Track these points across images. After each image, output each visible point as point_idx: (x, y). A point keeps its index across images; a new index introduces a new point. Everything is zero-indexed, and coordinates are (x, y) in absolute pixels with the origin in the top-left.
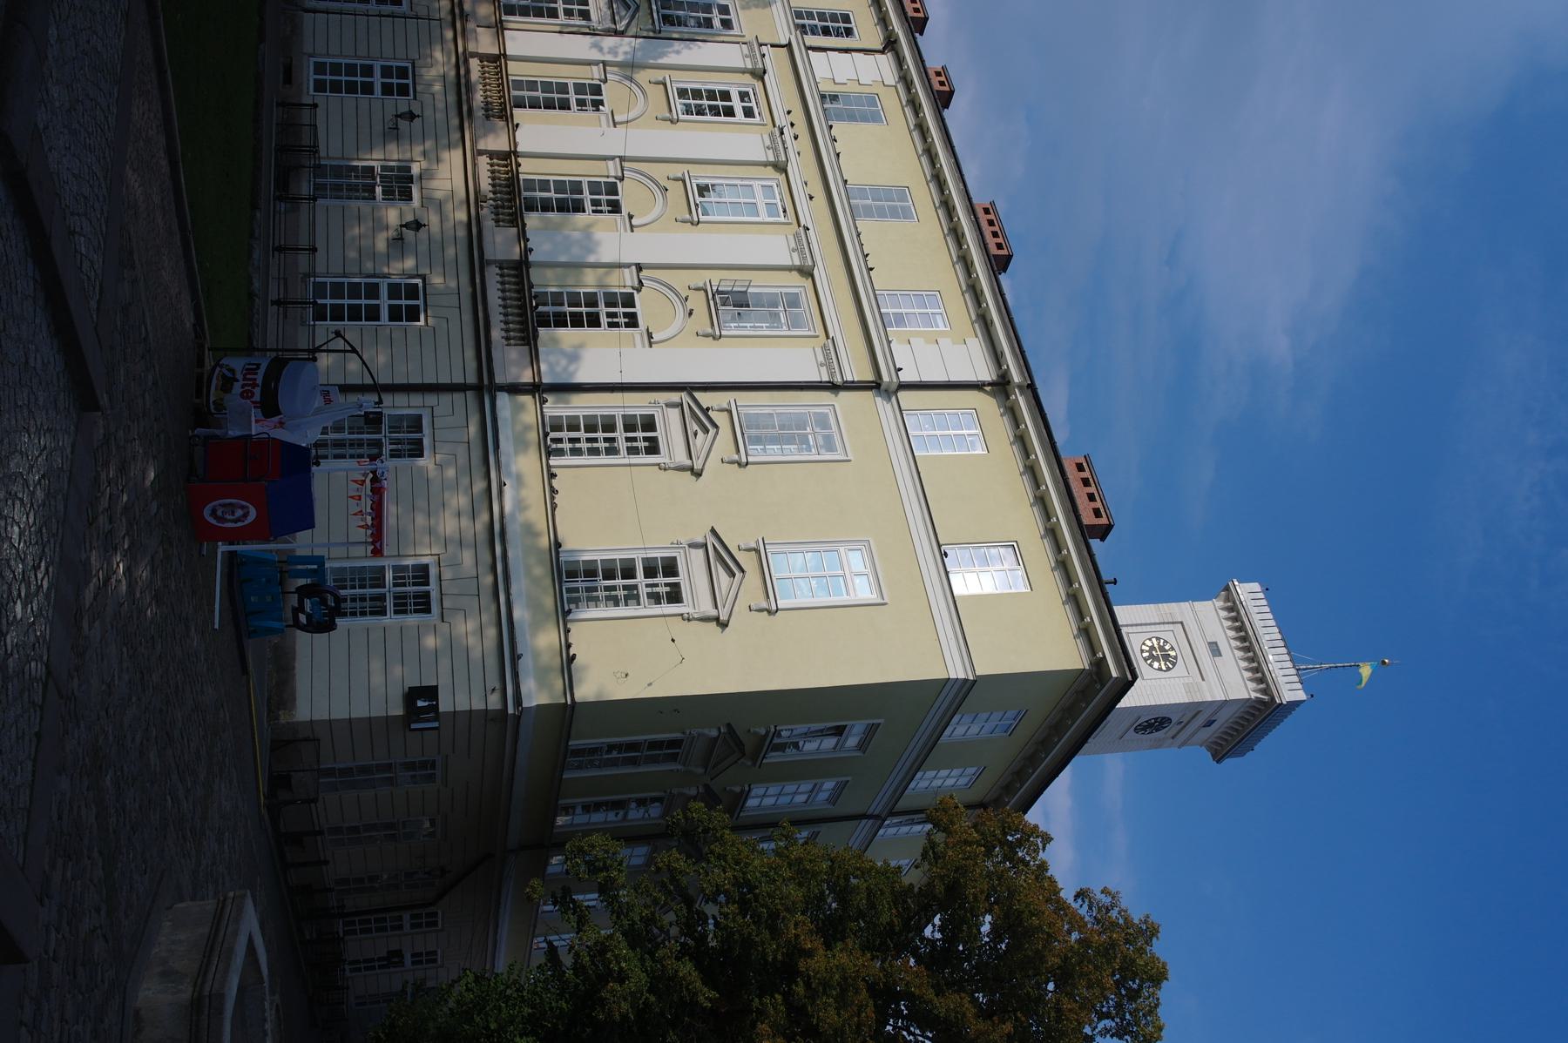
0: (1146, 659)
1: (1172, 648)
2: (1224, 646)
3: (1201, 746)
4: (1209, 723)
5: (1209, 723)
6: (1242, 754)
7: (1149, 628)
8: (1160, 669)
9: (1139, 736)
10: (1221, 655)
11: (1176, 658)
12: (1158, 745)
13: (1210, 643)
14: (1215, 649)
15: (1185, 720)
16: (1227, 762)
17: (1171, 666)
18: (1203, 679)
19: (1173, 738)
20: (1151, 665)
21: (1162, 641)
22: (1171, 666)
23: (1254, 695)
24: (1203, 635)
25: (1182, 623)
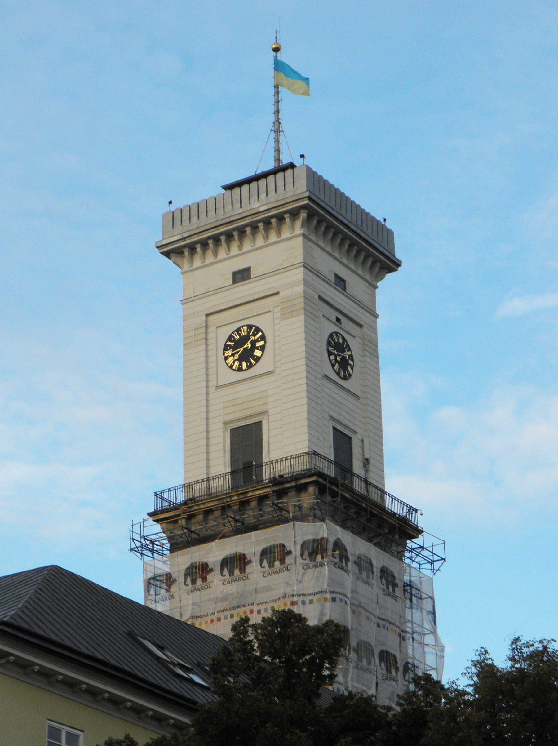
0: (250, 366)
1: (238, 330)
2: (239, 264)
4: (340, 282)
6: (389, 234)
7: (212, 359)
8: (263, 348)
9: (356, 373)
11: (250, 327)
13: (235, 281)
15: (333, 315)
16: (398, 255)
17: (260, 334)
20: (257, 359)
21: (228, 343)
22: (260, 334)
23: (298, 230)
25: (207, 315)
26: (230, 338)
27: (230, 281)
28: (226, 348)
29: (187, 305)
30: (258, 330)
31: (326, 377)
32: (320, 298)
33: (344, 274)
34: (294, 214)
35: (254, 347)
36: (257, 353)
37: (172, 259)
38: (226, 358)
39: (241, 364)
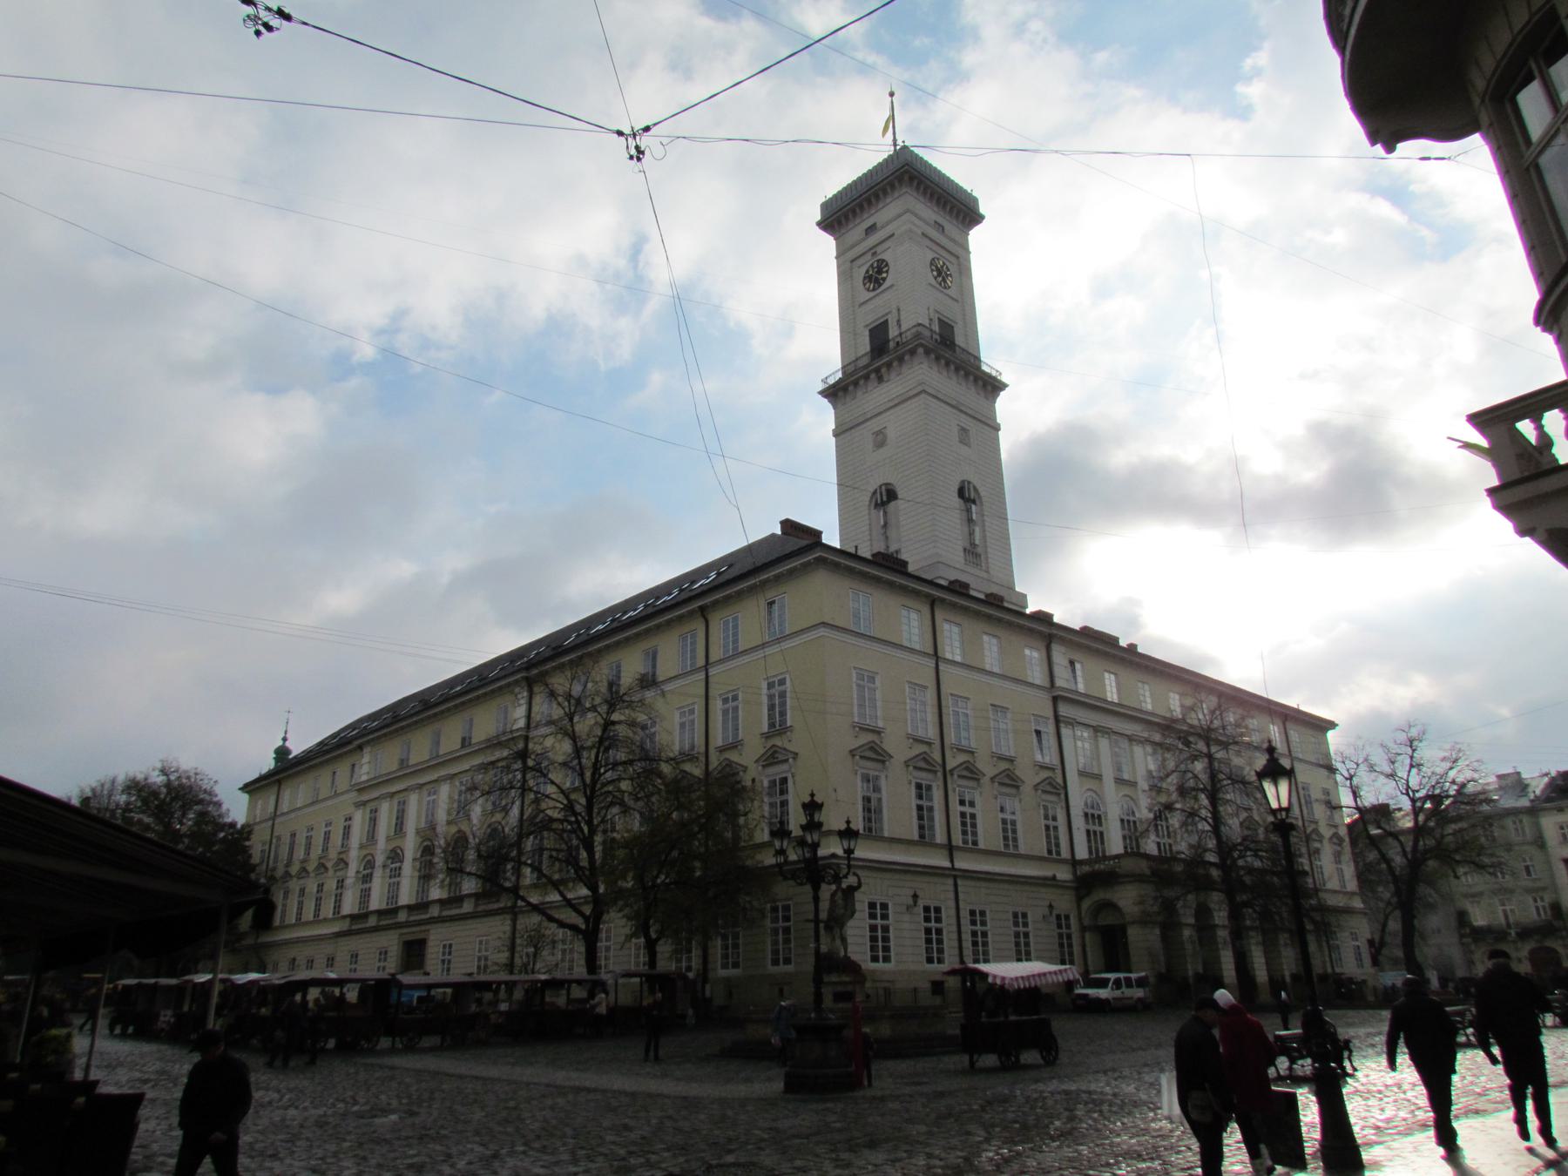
0: (880, 285)
1: (872, 265)
5: (940, 227)
6: (975, 200)
8: (887, 272)
10: (874, 225)
11: (878, 261)
12: (965, 270)
14: (871, 229)
18: (893, 235)
19: (958, 257)
20: (884, 279)
24: (864, 240)
25: (852, 261)
26: (867, 272)
28: (865, 278)
30: (883, 261)
31: (930, 284)
32: (923, 234)
33: (940, 220)
34: (900, 179)
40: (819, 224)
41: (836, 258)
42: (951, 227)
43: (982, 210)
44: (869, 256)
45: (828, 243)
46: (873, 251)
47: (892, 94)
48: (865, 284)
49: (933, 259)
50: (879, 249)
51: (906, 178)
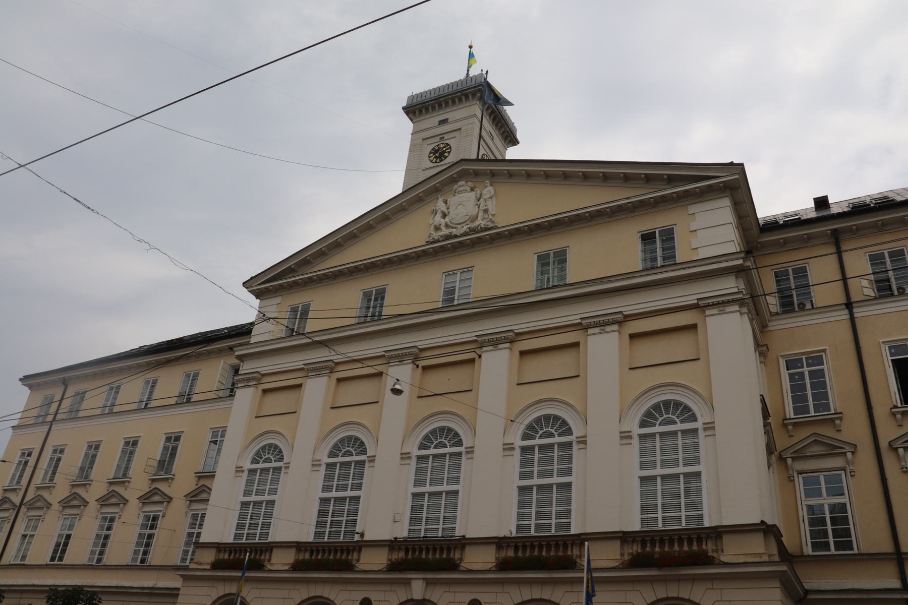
0: (440, 161)
1: (438, 145)
3: (507, 150)
8: (449, 153)
13: (439, 124)
14: (443, 122)
18: (460, 129)
20: (446, 157)
24: (435, 127)
25: (423, 139)
27: (437, 124)
28: (430, 153)
29: (414, 136)
30: (448, 144)
34: (474, 95)
35: (445, 152)
36: (446, 154)
37: (410, 115)
38: (430, 157)
39: (437, 160)
40: (404, 108)
41: (412, 134)
42: (498, 141)
43: (519, 136)
44: (437, 139)
45: (407, 125)
46: (441, 136)
47: (471, 47)
48: (430, 157)
49: (484, 154)
50: (446, 137)
51: (479, 95)
